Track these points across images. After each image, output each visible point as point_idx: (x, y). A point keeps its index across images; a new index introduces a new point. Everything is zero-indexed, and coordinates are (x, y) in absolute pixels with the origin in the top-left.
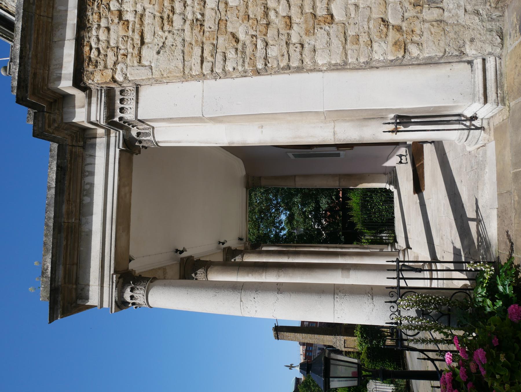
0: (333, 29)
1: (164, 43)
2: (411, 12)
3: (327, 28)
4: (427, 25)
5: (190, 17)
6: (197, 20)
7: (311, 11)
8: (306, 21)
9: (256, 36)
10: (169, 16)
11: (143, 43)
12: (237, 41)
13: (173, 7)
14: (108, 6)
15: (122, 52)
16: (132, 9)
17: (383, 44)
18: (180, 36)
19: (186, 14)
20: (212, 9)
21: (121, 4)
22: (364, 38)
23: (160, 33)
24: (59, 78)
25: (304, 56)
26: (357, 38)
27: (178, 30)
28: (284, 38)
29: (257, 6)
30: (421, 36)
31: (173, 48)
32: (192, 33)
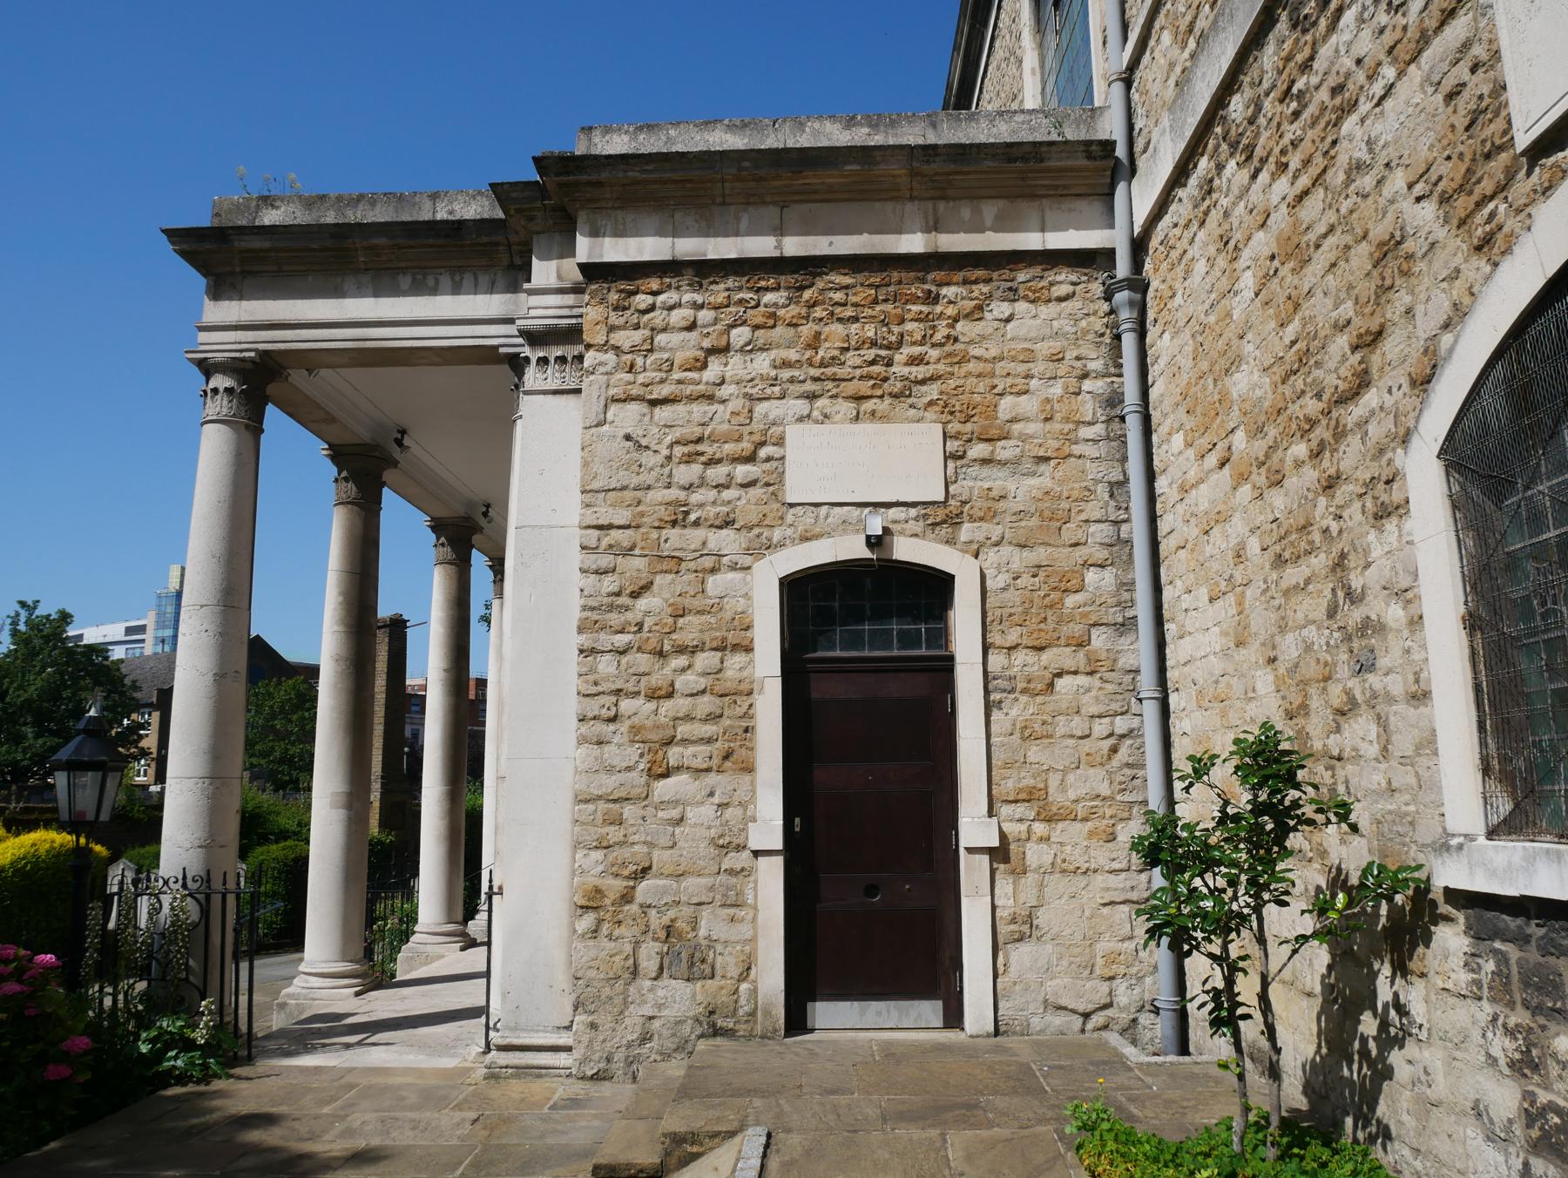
0: (637, 779)
1: (647, 447)
2: (656, 921)
3: (641, 766)
4: (628, 948)
5: (695, 498)
6: (687, 513)
7: (679, 737)
8: (657, 727)
9: (640, 630)
10: (702, 454)
11: (654, 403)
12: (635, 595)
13: (719, 461)
14: (739, 322)
15: (639, 361)
16: (728, 375)
17: (600, 868)
18: (657, 480)
19: (701, 491)
20: (704, 543)
21: (741, 350)
22: (614, 834)
23: (668, 440)
24: (595, 233)
25: (592, 722)
26: (619, 821)
27: (670, 475)
28: (630, 687)
29: (701, 631)
30: (610, 937)
31: (635, 468)
32: (661, 504)
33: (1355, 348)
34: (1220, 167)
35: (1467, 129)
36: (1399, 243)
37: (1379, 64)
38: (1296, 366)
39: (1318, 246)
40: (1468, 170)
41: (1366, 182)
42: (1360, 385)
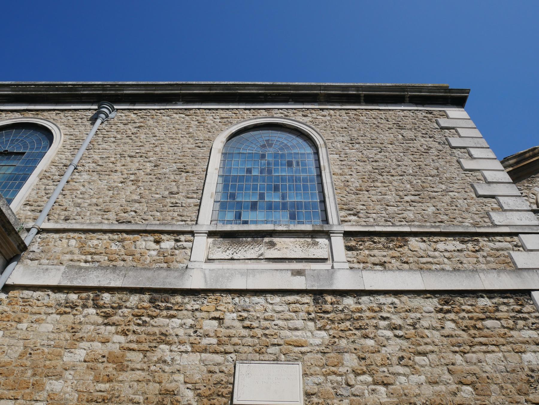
34: (85, 306)
35: (214, 384)
36: (175, 395)
37: (186, 343)
38: (100, 400)
39: (133, 370)
40: (211, 394)
41: (167, 368)
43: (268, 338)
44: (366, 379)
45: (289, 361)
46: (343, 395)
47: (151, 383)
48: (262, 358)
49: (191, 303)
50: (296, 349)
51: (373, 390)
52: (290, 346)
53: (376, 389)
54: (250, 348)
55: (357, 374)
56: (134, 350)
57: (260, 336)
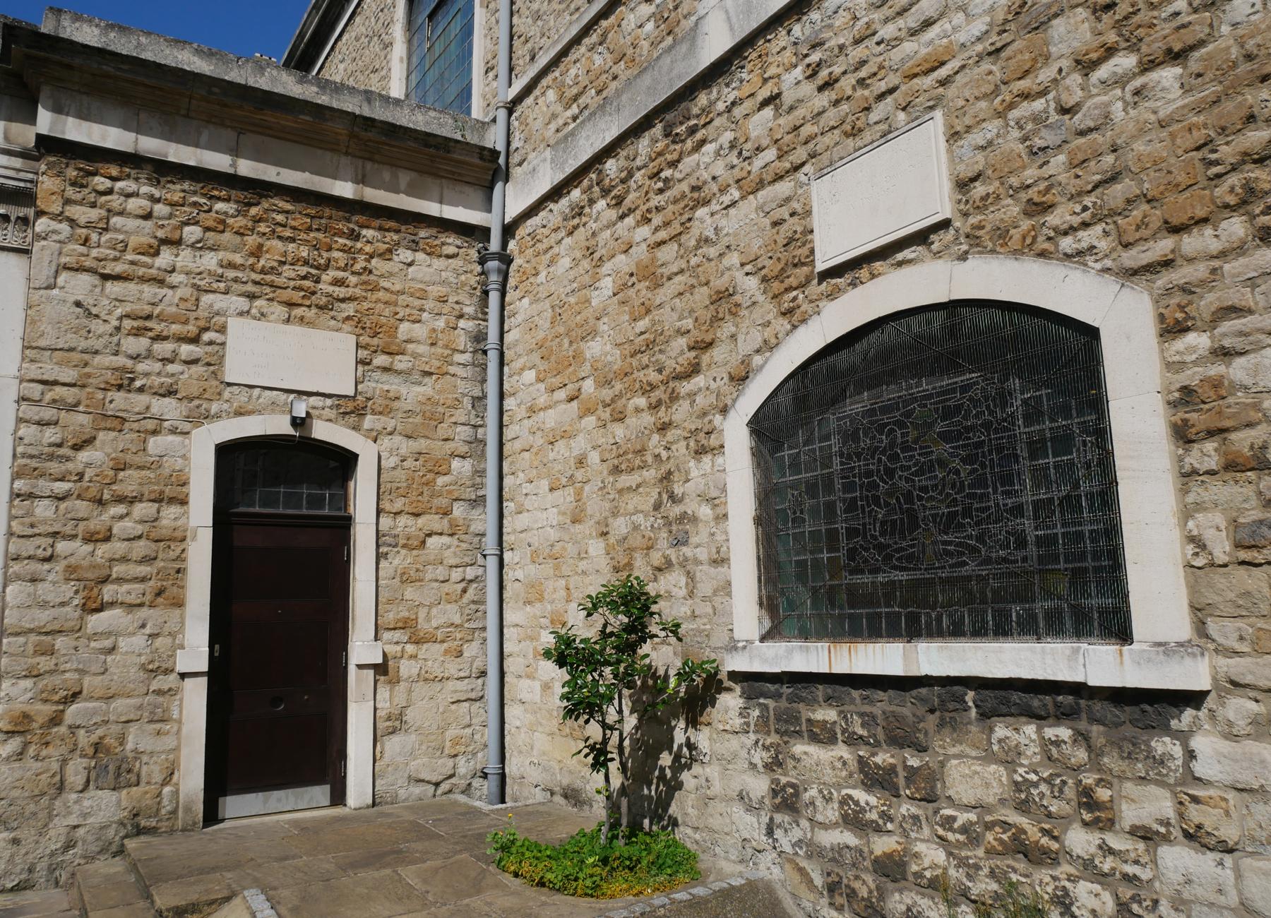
0: (71, 612)
1: (97, 316)
2: (83, 739)
3: (76, 602)
4: (55, 766)
5: (142, 367)
6: (132, 380)
7: (114, 576)
8: (94, 567)
9: (80, 480)
10: (151, 330)
11: (106, 277)
12: (77, 447)
13: (166, 338)
14: (192, 221)
15: (94, 237)
16: (178, 265)
17: (29, 695)
18: (106, 347)
19: (147, 362)
20: (148, 408)
21: (192, 246)
22: (45, 663)
23: (119, 312)
24: (58, 109)
25: (26, 562)
26: (51, 652)
27: (118, 344)
28: (68, 530)
29: (140, 484)
30: (36, 758)
31: (84, 333)
32: (108, 368)
33: (691, 348)
34: (592, 202)
35: (784, 246)
36: (731, 295)
37: (729, 186)
38: (644, 348)
39: (669, 279)
41: (712, 252)
42: (692, 371)
43: (868, 86)
44: (1116, 69)
45: (917, 118)
46: (1048, 147)
47: (697, 290)
48: (860, 143)
49: (721, 95)
50: (928, 81)
51: (1137, 93)
52: (915, 80)
53: (1144, 86)
54: (836, 132)
55: (1086, 65)
56: (664, 242)
57: (850, 93)
